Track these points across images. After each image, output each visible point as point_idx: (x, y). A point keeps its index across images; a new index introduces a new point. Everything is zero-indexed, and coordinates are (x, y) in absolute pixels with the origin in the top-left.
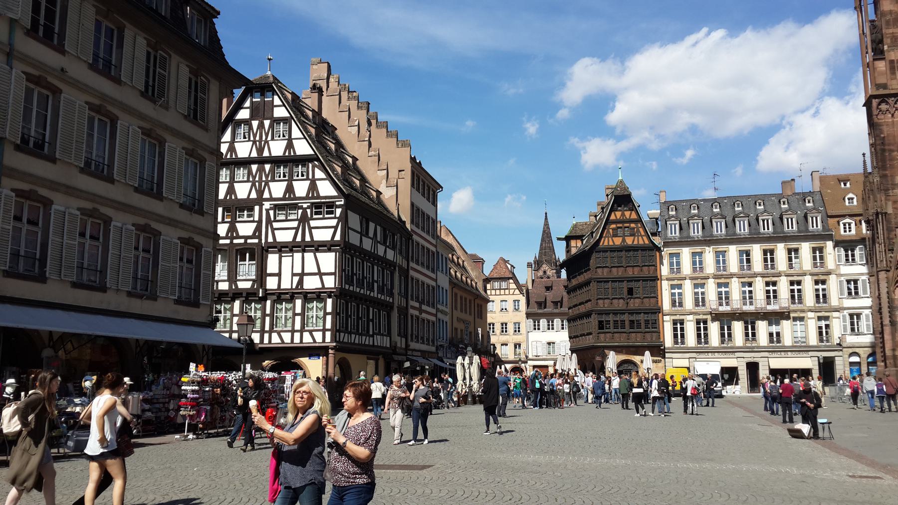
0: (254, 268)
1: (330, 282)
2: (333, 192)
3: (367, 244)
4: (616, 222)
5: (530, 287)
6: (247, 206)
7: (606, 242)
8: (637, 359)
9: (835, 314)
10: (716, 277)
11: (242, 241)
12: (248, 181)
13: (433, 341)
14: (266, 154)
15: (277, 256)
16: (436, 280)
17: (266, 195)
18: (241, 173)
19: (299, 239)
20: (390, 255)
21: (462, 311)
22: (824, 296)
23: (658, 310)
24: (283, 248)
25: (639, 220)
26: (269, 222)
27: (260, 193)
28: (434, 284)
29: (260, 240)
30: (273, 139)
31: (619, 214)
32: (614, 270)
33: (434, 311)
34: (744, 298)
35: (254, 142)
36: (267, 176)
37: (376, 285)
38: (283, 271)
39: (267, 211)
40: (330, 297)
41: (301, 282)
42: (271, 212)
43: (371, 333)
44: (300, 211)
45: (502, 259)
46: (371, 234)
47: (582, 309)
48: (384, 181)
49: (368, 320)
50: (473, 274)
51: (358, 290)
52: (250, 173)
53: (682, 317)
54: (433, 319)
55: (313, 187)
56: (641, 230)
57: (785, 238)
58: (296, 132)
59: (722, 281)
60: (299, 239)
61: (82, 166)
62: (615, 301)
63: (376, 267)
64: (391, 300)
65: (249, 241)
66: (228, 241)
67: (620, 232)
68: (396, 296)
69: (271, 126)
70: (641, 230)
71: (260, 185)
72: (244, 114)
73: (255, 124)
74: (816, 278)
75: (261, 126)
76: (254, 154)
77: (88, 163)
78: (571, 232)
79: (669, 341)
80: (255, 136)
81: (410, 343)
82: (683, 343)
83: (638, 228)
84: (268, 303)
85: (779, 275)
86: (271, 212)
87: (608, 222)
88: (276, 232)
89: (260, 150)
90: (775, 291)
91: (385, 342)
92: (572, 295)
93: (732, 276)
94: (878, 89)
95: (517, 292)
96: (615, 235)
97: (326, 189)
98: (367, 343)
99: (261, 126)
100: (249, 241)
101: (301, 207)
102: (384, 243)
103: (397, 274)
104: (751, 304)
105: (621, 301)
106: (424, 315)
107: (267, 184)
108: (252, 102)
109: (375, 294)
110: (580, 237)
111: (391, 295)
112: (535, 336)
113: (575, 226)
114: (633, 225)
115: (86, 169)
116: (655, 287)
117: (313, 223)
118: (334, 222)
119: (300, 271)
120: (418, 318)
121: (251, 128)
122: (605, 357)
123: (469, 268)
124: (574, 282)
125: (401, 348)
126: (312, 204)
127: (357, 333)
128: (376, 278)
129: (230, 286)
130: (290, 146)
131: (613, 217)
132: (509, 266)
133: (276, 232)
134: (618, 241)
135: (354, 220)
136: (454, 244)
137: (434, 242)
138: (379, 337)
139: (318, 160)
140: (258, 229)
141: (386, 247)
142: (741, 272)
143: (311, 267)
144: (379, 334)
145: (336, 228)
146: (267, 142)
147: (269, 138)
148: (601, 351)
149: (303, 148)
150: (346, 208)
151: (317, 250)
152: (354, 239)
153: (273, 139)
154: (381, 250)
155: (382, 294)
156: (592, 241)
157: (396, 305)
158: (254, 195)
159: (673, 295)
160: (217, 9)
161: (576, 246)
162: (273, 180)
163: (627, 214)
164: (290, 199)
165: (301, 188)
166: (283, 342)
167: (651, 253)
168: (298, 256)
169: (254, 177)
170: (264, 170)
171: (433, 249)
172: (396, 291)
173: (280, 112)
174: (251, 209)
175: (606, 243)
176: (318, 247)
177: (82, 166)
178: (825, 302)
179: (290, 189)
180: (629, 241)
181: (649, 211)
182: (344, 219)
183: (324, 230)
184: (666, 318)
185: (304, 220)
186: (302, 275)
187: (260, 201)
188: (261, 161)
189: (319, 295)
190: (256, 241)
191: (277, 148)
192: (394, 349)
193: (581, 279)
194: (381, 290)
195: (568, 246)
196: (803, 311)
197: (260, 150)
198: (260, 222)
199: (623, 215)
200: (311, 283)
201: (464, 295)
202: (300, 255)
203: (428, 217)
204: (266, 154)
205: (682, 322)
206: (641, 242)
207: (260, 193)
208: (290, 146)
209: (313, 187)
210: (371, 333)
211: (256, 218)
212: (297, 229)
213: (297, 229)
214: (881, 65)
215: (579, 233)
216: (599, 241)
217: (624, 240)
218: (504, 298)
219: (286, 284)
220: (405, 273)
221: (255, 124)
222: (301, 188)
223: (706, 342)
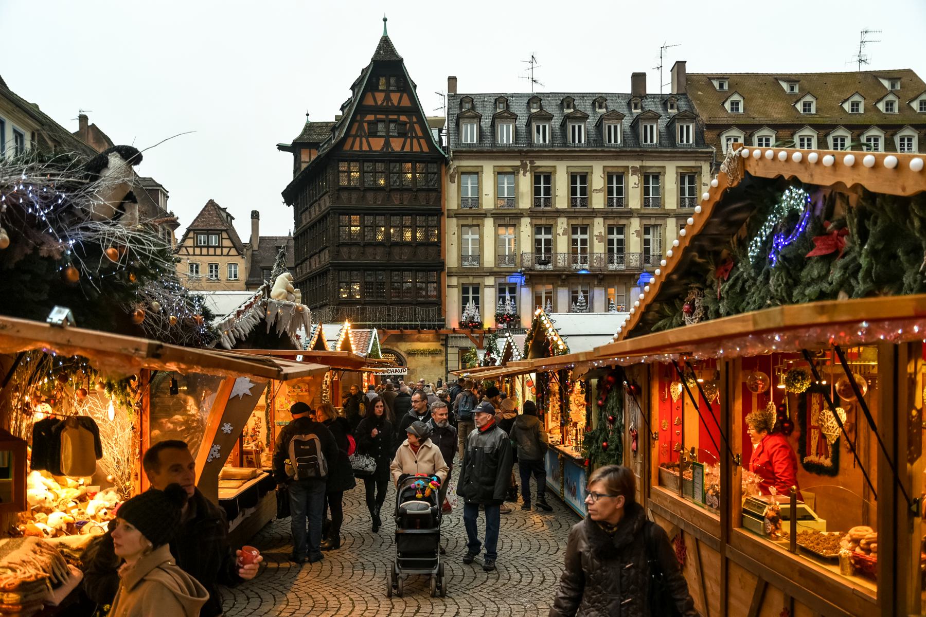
4: (376, 110)
10: (532, 214)
25: (415, 109)
31: (380, 97)
34: (575, 252)
45: (211, 202)
53: (477, 280)
56: (417, 127)
57: (642, 155)
59: (543, 222)
62: (369, 250)
67: (381, 126)
70: (417, 127)
78: (301, 136)
83: (412, 124)
85: (630, 214)
90: (620, 242)
93: (560, 213)
95: (233, 252)
96: (373, 134)
104: (584, 261)
110: (315, 146)
113: (310, 127)
114: (403, 118)
132: (224, 215)
134: (377, 144)
142: (572, 209)
159: (461, 242)
163: (395, 97)
167: (433, 168)
175: (356, 147)
180: (396, 145)
184: (454, 281)
193: (315, 212)
199: (387, 98)
205: (476, 290)
206: (416, 148)
215: (315, 138)
216: (343, 141)
217: (387, 144)
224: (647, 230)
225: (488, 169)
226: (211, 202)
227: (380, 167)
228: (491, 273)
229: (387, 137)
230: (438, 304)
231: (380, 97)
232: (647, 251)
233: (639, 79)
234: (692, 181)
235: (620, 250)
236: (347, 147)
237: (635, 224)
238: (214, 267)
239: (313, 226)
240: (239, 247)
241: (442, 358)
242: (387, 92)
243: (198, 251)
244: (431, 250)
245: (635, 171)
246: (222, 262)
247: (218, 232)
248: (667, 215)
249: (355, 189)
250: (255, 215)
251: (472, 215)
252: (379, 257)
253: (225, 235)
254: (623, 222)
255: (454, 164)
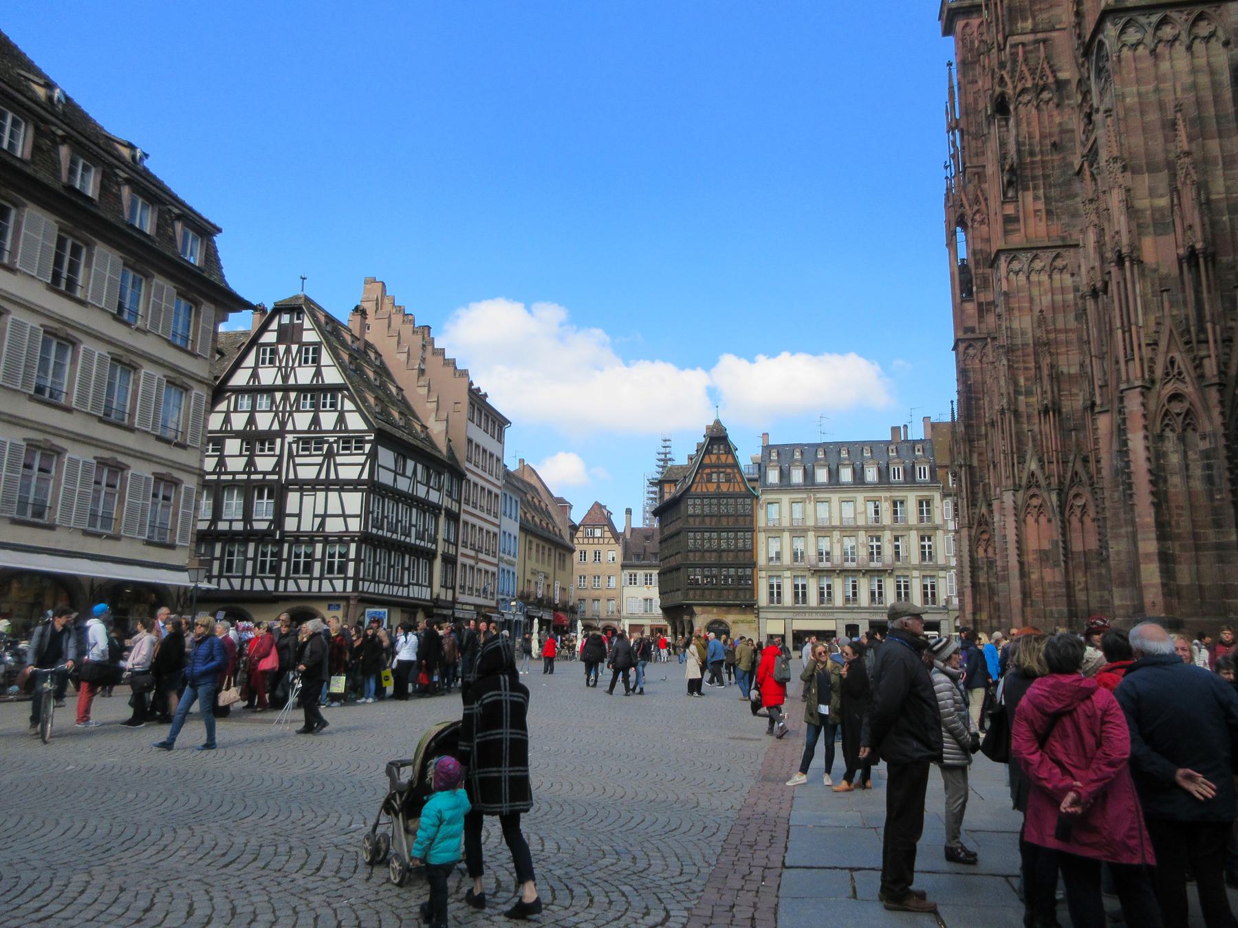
0: (271, 507)
1: (355, 525)
2: (364, 427)
3: (403, 484)
4: (711, 466)
5: (628, 536)
6: (267, 438)
7: (698, 489)
8: (729, 618)
9: (942, 574)
11: (260, 477)
12: (271, 411)
13: (492, 594)
14: (292, 381)
15: (298, 494)
16: (499, 526)
17: (289, 427)
18: (263, 402)
19: (323, 476)
20: (434, 497)
21: (537, 561)
22: (930, 553)
23: (753, 565)
24: (304, 486)
25: (736, 465)
26: (291, 456)
27: (283, 424)
28: (496, 530)
29: (280, 477)
30: (300, 365)
31: (714, 458)
32: (707, 520)
33: (495, 561)
35: (280, 368)
36: (291, 406)
37: (413, 529)
38: (304, 511)
39: (290, 444)
40: (353, 541)
41: (322, 524)
42: (294, 446)
43: (406, 582)
44: (326, 446)
45: (597, 504)
46: (409, 472)
47: (673, 562)
48: (434, 415)
49: (403, 569)
50: (557, 519)
51: (389, 535)
52: (273, 401)
54: (495, 569)
55: (341, 419)
58: (326, 358)
60: (323, 476)
61: (32, 392)
63: (414, 511)
64: (434, 547)
65: (268, 477)
66: (245, 477)
67: (714, 476)
68: (440, 542)
69: (299, 351)
71: (283, 416)
72: (270, 337)
73: (282, 348)
74: (922, 533)
75: (288, 351)
76: (279, 382)
77: (40, 390)
79: (763, 598)
80: (280, 362)
81: (457, 595)
82: (779, 602)
84: (286, 546)
85: (883, 528)
86: (294, 446)
87: (702, 466)
88: (298, 468)
89: (285, 378)
90: (878, 547)
91: (425, 594)
92: (664, 545)
93: (834, 528)
94: (965, 332)
95: (612, 541)
96: (709, 481)
97: (355, 422)
98: (400, 594)
99: (288, 351)
100: (268, 477)
101: (327, 442)
102: (427, 484)
103: (442, 519)
105: (714, 554)
106: (481, 565)
107: (291, 414)
108: (280, 325)
109: (412, 540)
110: (675, 482)
111: (435, 541)
112: (630, 591)
114: (729, 470)
115: (39, 395)
116: (752, 539)
117: (339, 460)
118: (362, 459)
119: (322, 512)
120: (472, 568)
121: (274, 352)
122: (692, 614)
123: (553, 514)
124: (667, 532)
125: (446, 601)
126: (339, 438)
127: (387, 583)
128: (414, 522)
129: (245, 526)
130: (318, 373)
131: (707, 461)
133: (298, 468)
134: (712, 488)
135: (386, 457)
136: (538, 485)
137: (499, 483)
138: (416, 588)
139: (348, 389)
140: (279, 464)
141: (429, 487)
143: (334, 508)
144: (417, 584)
145: (363, 465)
146: (293, 368)
147: (296, 364)
148: (688, 610)
149: (332, 376)
150: (375, 444)
151: (341, 490)
152: (386, 478)
153: (300, 365)
154: (421, 491)
155: (422, 539)
156: (685, 487)
157: (440, 552)
158: (276, 427)
160: (218, 225)
161: (670, 492)
162: (298, 410)
163: (723, 458)
164: (315, 432)
165: (328, 420)
166: (299, 590)
167: (748, 501)
168: (321, 495)
169: (277, 407)
170: (288, 398)
171: (495, 490)
172: (440, 537)
173: (310, 336)
174: (272, 443)
176: (344, 486)
177: (32, 392)
178: (931, 559)
179: (316, 421)
180: (724, 488)
181: (747, 455)
182: (373, 456)
183: (350, 467)
184: (763, 574)
185: (330, 455)
186: (324, 516)
187: (282, 433)
188: (286, 389)
189: (341, 539)
190: (276, 477)
191: (304, 376)
192: (436, 602)
193: (673, 528)
194: (420, 536)
195: (661, 490)
196: (907, 569)
197: (285, 378)
198: (281, 456)
199: (718, 458)
200: (334, 526)
201: (541, 543)
202: (323, 493)
203: (491, 455)
204: (292, 381)
206: (737, 489)
207: (283, 424)
208: (318, 373)
209: (341, 419)
210: (406, 582)
211: (277, 452)
212: (321, 465)
213: (321, 465)
214: (970, 307)
216: (690, 487)
217: (718, 487)
218: (597, 547)
219: (306, 526)
220: (453, 517)
221: (282, 348)
222: (328, 420)
223: (804, 601)
224: (896, 539)
225: (785, 498)
226: (597, 504)
227: (714, 501)
228: (789, 569)
229: (719, 482)
230: (752, 590)
231: (714, 458)
232: (897, 554)
233: (895, 430)
234: (928, 505)
235: (879, 553)
236: (693, 489)
237: (887, 536)
238: (597, 555)
239: (672, 536)
240: (616, 536)
241: (754, 625)
242: (718, 455)
243: (586, 541)
244: (748, 554)
245: (886, 499)
246: (602, 549)
247: (602, 526)
248: (910, 528)
249: (698, 516)
250: (629, 511)
251: (775, 532)
252: (712, 558)
253: (606, 528)
254: (879, 533)
255: (763, 498)
